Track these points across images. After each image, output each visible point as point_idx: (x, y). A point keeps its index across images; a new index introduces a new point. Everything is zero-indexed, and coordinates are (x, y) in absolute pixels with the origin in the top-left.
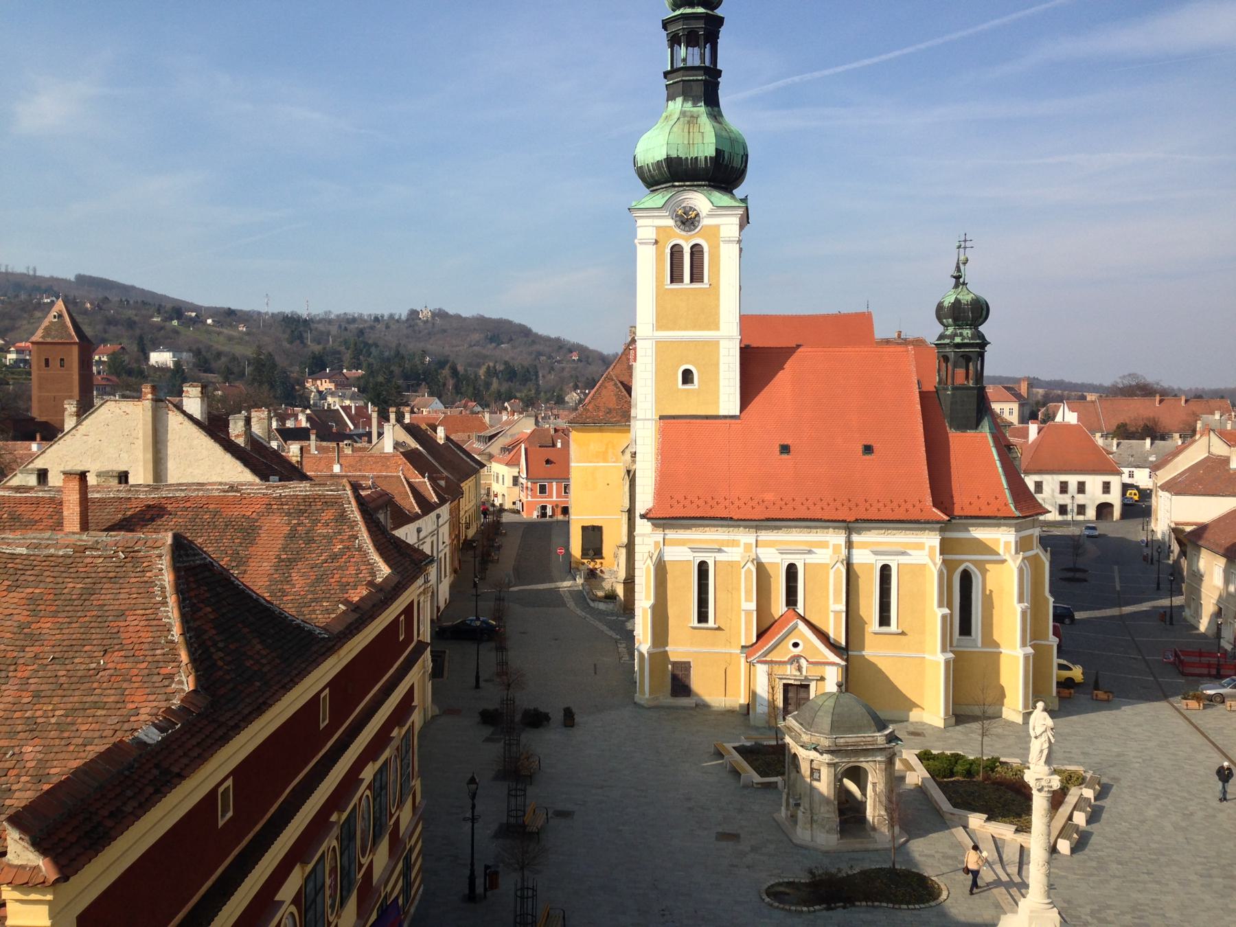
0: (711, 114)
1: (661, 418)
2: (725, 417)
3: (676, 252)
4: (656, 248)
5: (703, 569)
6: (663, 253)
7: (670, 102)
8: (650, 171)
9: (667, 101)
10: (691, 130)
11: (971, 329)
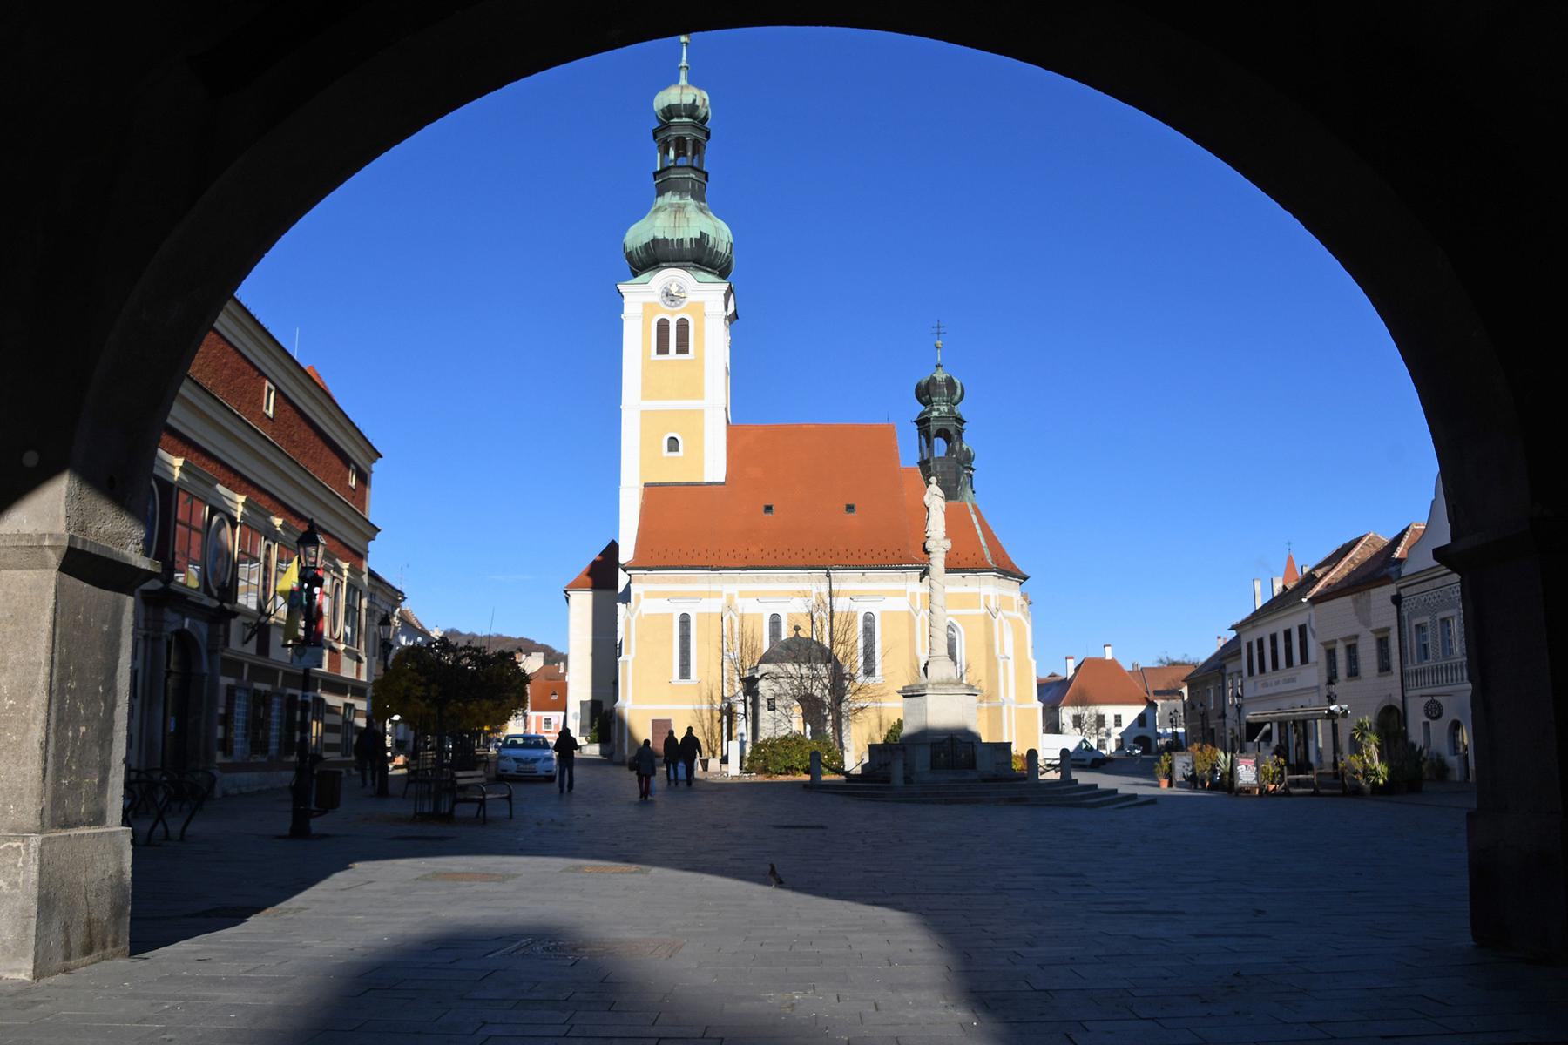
0: (696, 206)
1: (646, 485)
2: (710, 484)
3: (663, 327)
4: (643, 321)
5: (685, 621)
7: (659, 198)
8: (638, 254)
9: (657, 197)
10: (677, 216)
11: (947, 405)
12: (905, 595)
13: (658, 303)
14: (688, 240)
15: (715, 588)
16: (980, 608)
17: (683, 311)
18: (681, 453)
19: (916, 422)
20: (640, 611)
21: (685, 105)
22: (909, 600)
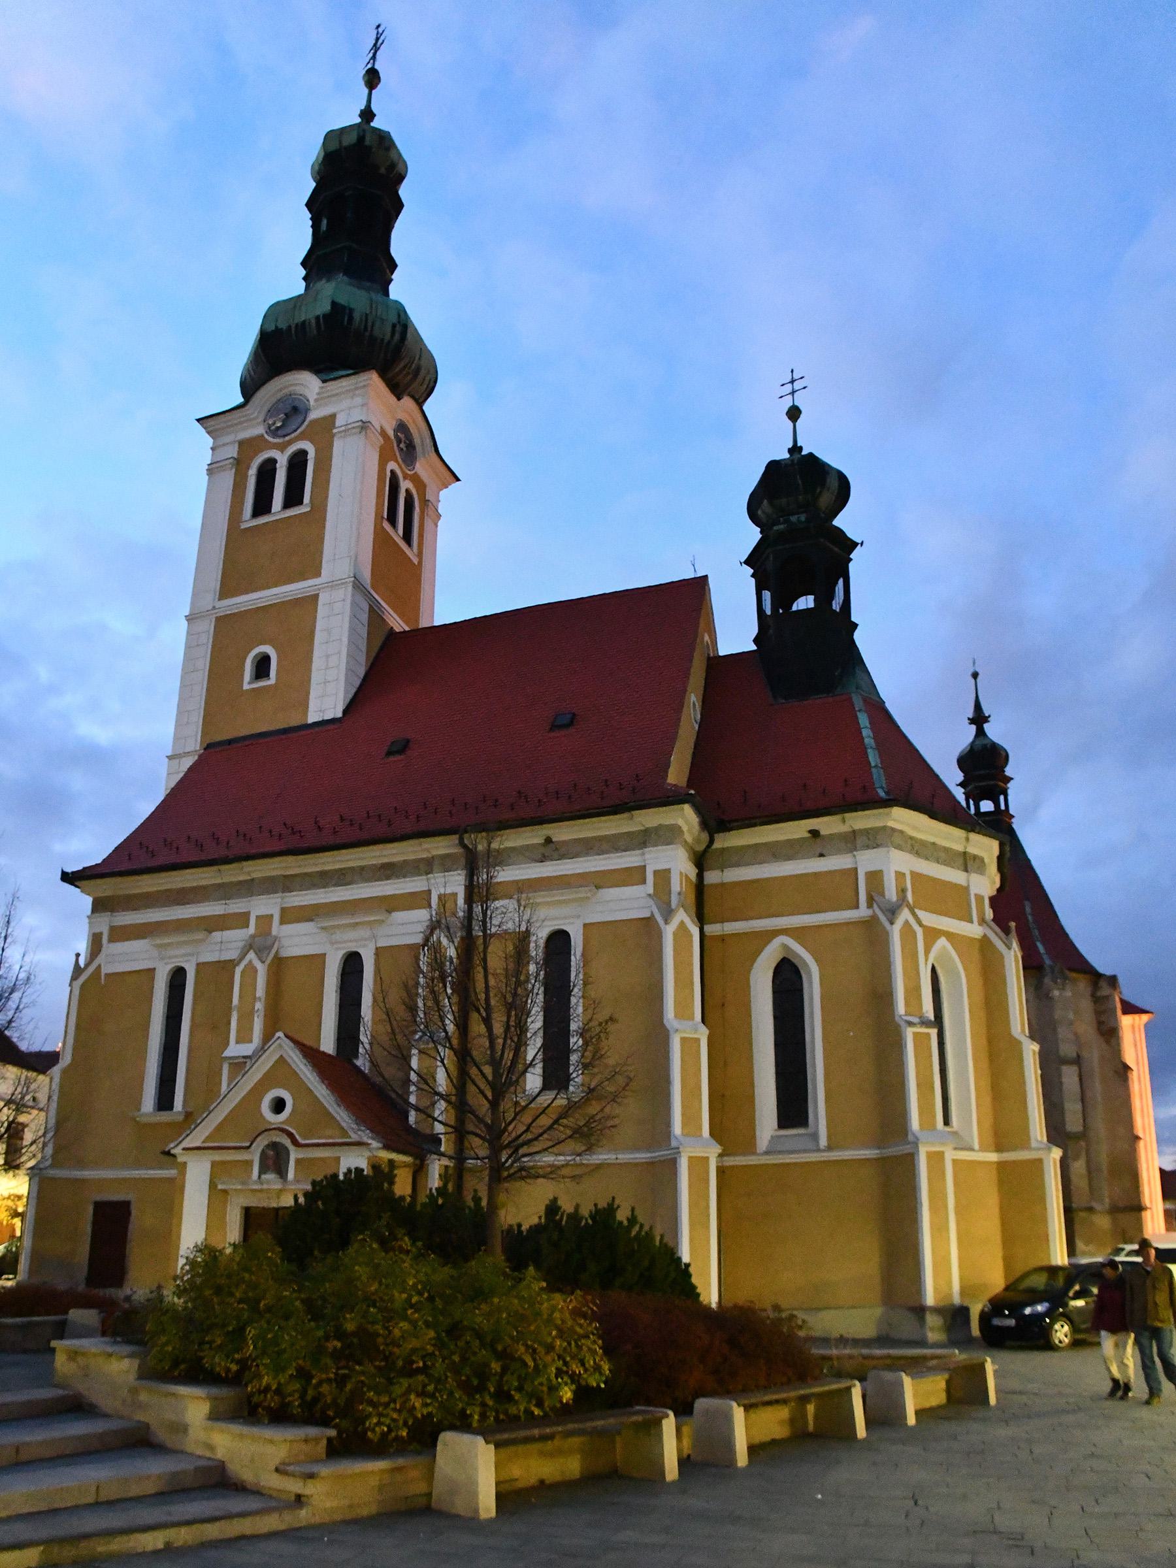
3: (267, 472)
6: (246, 477)
12: (643, 881)
13: (262, 436)
14: (313, 321)
15: (236, 906)
16: (857, 907)
17: (302, 437)
18: (273, 679)
19: (747, 562)
20: (99, 966)
21: (345, 148)
22: (651, 891)
